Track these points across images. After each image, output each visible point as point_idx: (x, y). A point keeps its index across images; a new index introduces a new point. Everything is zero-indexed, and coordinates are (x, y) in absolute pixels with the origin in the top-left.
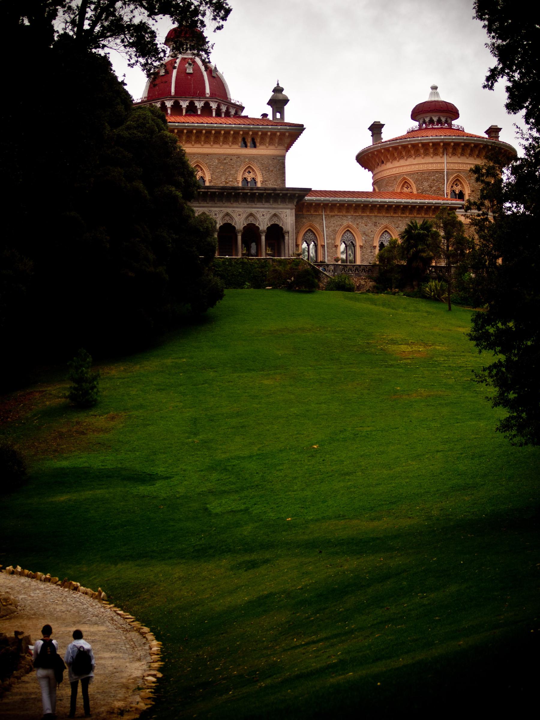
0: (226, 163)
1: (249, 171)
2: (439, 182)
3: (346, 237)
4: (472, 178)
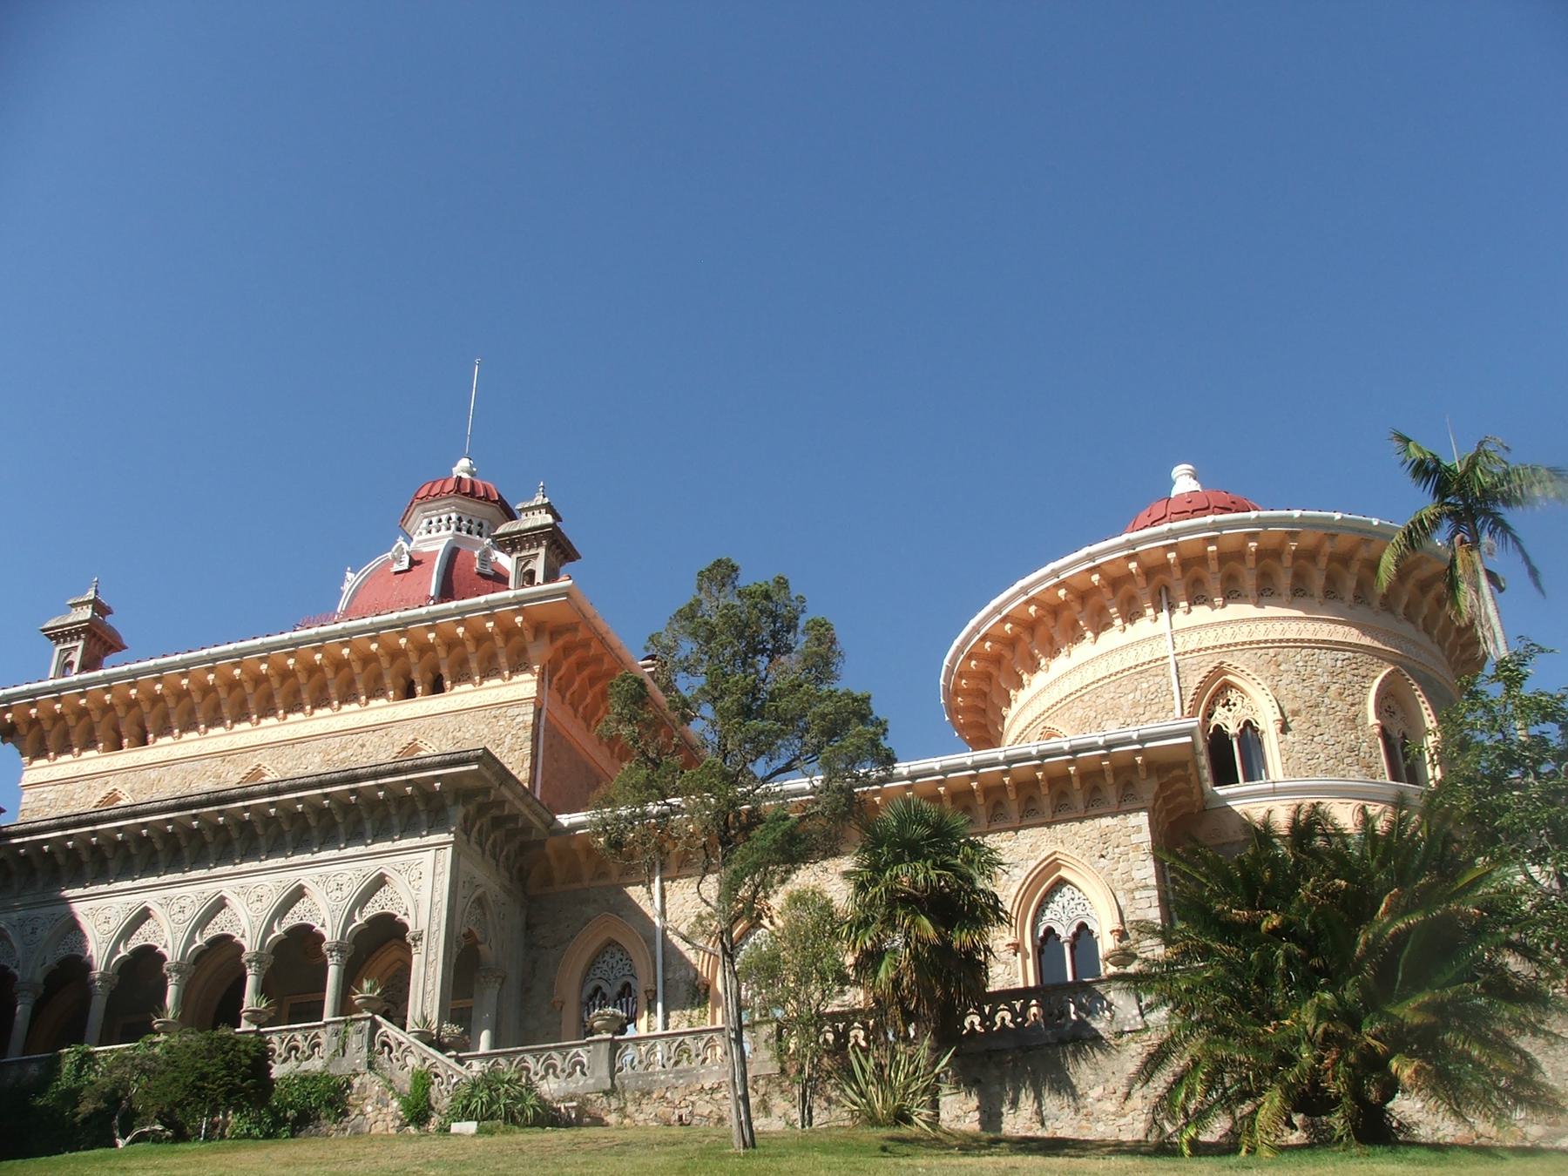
2: (1154, 708)
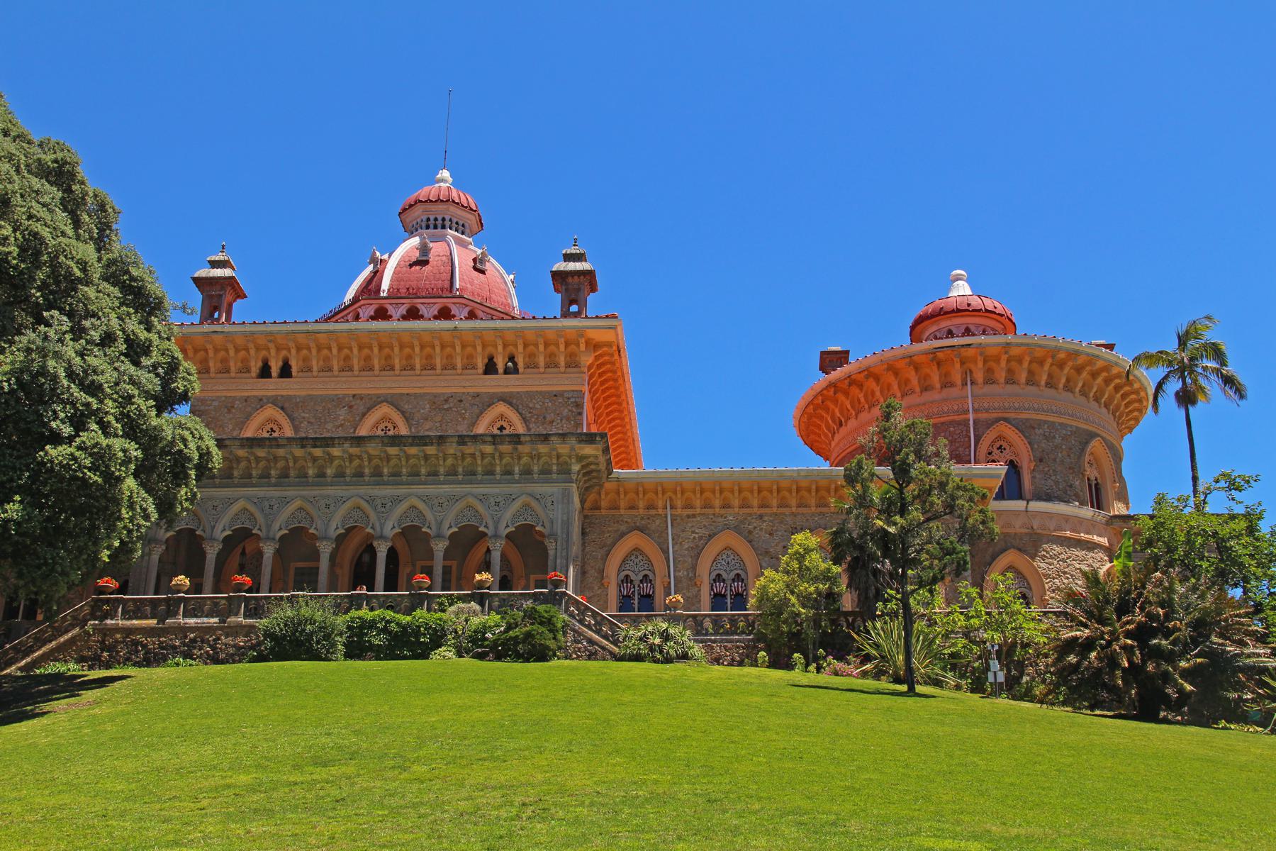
0: (447, 410)
1: (502, 426)
2: (957, 445)
3: (723, 563)
4: (1037, 430)
